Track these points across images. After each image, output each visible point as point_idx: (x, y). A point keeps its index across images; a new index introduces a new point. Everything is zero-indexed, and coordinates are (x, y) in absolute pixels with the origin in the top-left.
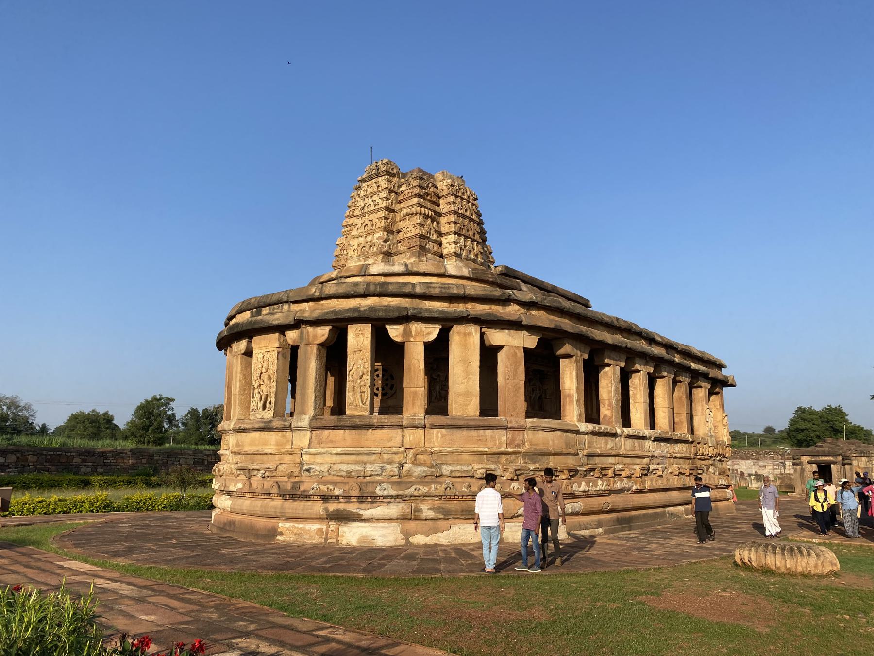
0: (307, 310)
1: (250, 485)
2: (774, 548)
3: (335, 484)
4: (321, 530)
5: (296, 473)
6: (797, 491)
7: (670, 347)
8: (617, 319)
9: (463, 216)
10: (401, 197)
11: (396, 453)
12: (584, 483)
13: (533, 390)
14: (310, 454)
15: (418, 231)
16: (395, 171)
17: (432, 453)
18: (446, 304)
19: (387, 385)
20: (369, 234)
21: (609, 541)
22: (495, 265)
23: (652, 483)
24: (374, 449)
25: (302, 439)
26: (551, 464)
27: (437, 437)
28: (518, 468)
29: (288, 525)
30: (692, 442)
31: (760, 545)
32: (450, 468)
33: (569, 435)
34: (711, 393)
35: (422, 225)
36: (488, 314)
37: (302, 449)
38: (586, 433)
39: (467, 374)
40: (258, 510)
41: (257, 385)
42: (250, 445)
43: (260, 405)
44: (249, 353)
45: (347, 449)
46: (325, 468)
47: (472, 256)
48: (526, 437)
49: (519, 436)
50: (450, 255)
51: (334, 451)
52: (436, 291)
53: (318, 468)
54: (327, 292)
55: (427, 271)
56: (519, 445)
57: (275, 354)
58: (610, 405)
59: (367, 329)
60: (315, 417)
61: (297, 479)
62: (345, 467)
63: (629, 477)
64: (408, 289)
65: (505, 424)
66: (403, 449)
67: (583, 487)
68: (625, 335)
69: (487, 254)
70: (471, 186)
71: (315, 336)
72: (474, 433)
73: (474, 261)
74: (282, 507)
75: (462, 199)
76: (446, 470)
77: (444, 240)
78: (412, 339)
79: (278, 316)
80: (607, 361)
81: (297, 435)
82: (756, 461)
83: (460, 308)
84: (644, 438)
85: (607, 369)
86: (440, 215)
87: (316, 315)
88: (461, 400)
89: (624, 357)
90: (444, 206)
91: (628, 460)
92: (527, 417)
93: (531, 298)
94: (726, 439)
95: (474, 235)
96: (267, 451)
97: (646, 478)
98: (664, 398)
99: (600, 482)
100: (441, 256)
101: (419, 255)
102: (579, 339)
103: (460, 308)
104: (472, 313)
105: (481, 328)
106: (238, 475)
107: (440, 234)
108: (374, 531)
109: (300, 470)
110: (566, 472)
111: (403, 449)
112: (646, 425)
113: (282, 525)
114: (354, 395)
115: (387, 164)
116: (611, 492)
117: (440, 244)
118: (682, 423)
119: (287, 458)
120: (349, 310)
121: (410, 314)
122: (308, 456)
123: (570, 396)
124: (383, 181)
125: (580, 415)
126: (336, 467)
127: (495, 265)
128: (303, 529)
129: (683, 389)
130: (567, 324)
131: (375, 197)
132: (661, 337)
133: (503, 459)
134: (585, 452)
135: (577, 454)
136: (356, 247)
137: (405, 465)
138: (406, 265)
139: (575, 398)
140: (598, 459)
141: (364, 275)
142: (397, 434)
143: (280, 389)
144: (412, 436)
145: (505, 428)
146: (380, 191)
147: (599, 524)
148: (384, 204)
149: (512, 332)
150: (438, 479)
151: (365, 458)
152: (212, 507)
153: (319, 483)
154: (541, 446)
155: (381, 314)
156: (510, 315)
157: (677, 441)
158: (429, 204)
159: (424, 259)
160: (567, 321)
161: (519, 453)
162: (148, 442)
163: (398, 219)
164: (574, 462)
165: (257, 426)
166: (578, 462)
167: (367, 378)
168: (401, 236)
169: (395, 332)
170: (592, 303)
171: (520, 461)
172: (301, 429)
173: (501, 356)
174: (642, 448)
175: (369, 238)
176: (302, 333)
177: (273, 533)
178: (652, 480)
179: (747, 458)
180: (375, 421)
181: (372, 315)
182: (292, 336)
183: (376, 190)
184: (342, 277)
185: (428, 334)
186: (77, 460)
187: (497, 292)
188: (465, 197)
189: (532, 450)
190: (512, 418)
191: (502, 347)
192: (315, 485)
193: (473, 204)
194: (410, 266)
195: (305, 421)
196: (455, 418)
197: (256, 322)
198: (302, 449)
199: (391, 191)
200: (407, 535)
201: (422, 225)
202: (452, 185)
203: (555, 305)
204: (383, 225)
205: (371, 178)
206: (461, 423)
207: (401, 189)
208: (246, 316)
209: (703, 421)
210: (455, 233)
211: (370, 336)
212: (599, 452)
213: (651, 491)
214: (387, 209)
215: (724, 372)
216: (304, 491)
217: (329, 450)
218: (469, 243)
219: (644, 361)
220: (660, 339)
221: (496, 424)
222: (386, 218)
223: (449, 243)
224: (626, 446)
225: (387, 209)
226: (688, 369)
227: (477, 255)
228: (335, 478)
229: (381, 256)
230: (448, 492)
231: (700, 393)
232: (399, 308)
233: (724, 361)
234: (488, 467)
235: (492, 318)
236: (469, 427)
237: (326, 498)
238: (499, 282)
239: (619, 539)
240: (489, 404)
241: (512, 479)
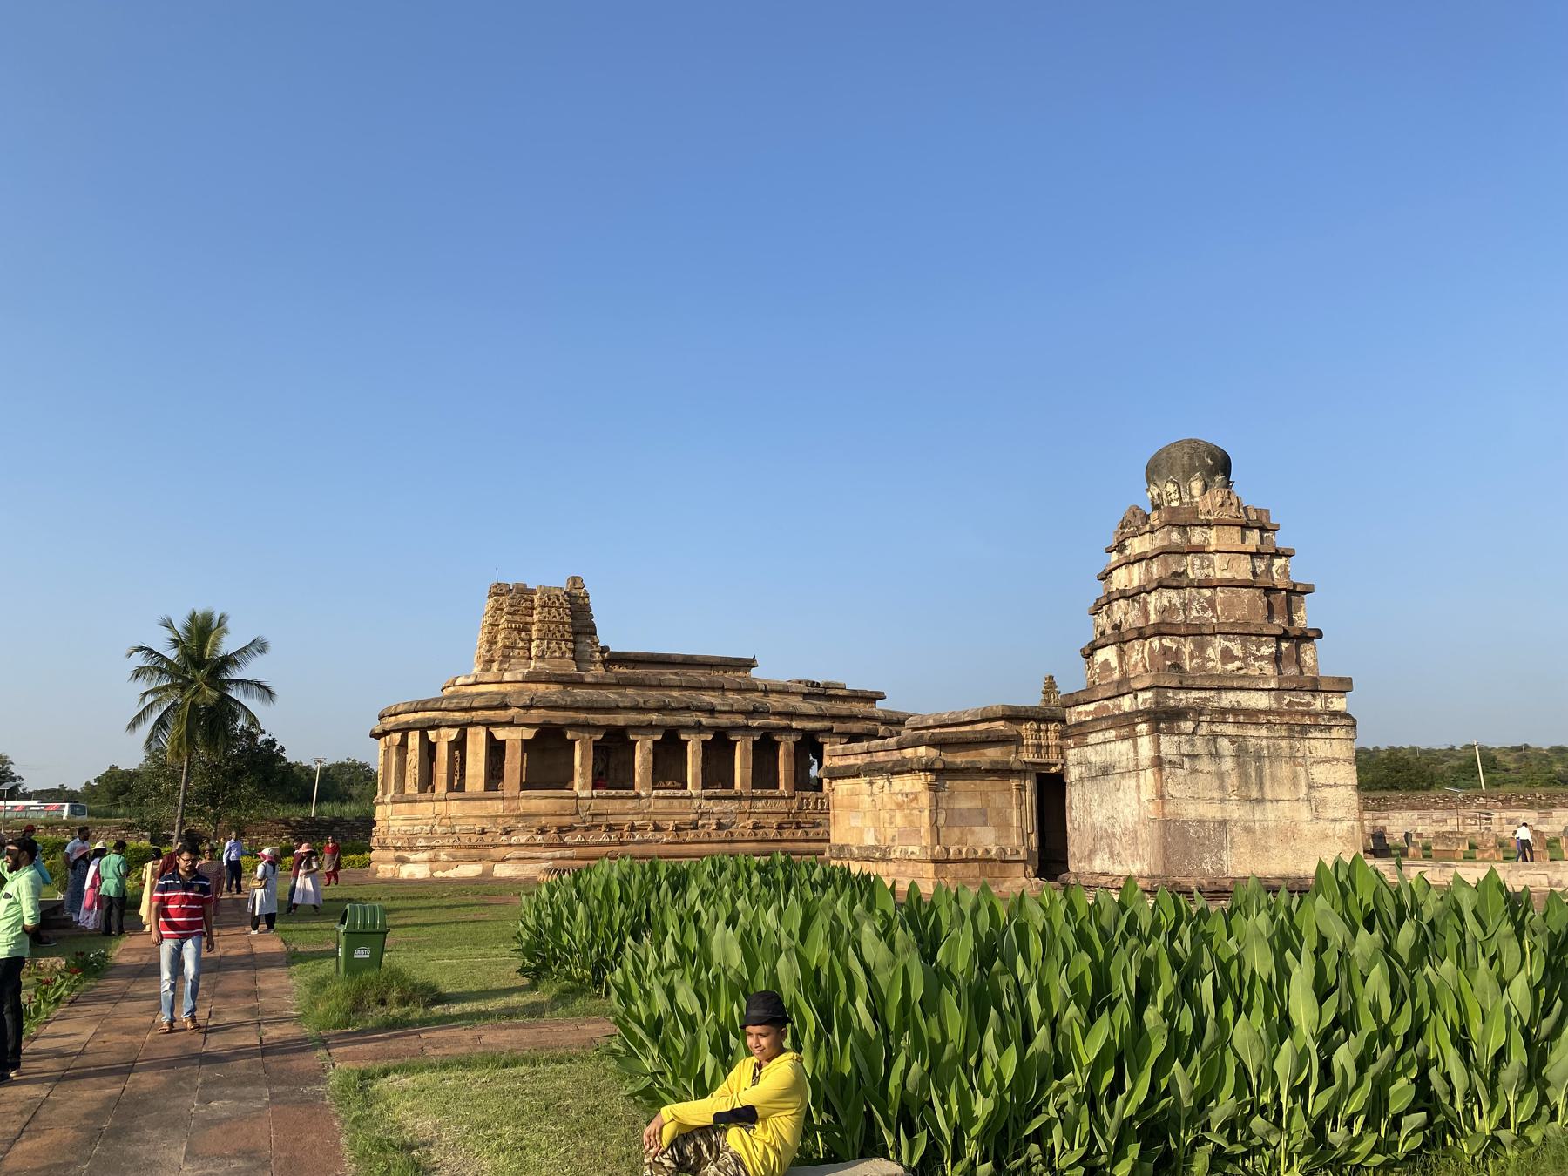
0: (391, 722)
39: (475, 761)
49: (514, 805)
73: (562, 657)
76: (457, 829)
84: (691, 797)
100: (530, 658)
108: (416, 870)
112: (695, 786)
113: (381, 867)
116: (622, 843)
135: (577, 813)
144: (440, 807)
158: (518, 618)
169: (432, 735)
171: (513, 822)
177: (377, 871)
195: (388, 799)
214: (492, 625)
218: (553, 645)
225: (492, 625)
226: (789, 729)
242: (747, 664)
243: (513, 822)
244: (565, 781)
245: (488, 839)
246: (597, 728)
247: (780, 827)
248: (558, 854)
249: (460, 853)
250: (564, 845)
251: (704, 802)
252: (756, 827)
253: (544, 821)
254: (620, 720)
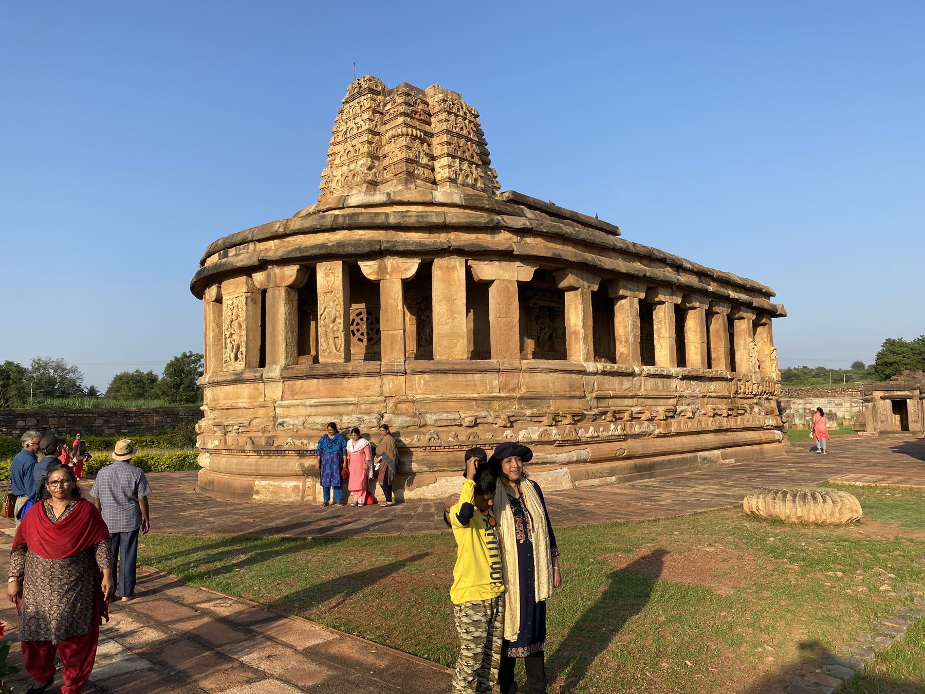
0: (272, 249)
1: (226, 441)
2: (785, 494)
3: (310, 437)
4: (297, 487)
5: (270, 428)
6: (869, 429)
7: (702, 274)
8: (634, 245)
9: (459, 136)
10: (387, 118)
11: (374, 403)
12: (592, 428)
13: (541, 329)
14: (283, 407)
15: (404, 155)
16: (379, 88)
17: (414, 401)
18: (426, 235)
19: (372, 329)
20: (352, 162)
21: (618, 491)
22: (501, 191)
23: (679, 425)
24: (351, 399)
25: (275, 391)
26: (552, 408)
27: (419, 382)
28: (511, 414)
29: (264, 483)
30: (731, 380)
31: (770, 491)
32: (434, 417)
33: (574, 376)
34: (756, 325)
35: (408, 148)
36: (473, 245)
37: (275, 402)
38: (596, 373)
39: (452, 312)
40: (234, 468)
41: (228, 334)
42: (225, 399)
43: (232, 355)
44: (219, 300)
45: (321, 400)
46: (299, 422)
47: (470, 181)
48: (522, 380)
49: (513, 380)
50: (444, 181)
51: (308, 402)
52: (412, 221)
53: (291, 422)
54: (292, 228)
55: (411, 200)
56: (513, 390)
57: (243, 300)
58: (627, 341)
59: (337, 267)
60: (286, 368)
61: (272, 434)
63: (651, 420)
64: (380, 220)
65: (497, 366)
66: (382, 398)
67: (591, 432)
68: (645, 262)
69: (491, 180)
70: (470, 101)
71: (283, 278)
72: (461, 378)
73: (473, 187)
74: (256, 465)
75: (457, 116)
76: (430, 419)
77: (437, 165)
78: (388, 277)
79: (240, 257)
80: (621, 292)
81: (268, 386)
82: (832, 399)
83: (442, 239)
84: (669, 377)
85: (623, 301)
86: (432, 135)
87: (280, 253)
88: (445, 342)
89: (644, 287)
90: (436, 125)
91: (650, 402)
92: (522, 359)
93: (524, 224)
94: (774, 376)
95: (472, 156)
96: (240, 405)
97: (672, 421)
98: (695, 332)
99: (612, 426)
100: (434, 182)
101: (406, 182)
102: (584, 268)
103: (442, 239)
104: (453, 243)
105: (467, 261)
106: (216, 432)
107: (432, 158)
109: (274, 425)
110: (569, 416)
111: (382, 398)
112: (672, 361)
113: (259, 483)
114: (327, 341)
115: (370, 80)
116: (626, 437)
117: (433, 170)
118: (719, 358)
119: (261, 412)
120: (315, 247)
121: (382, 248)
122: (281, 409)
123: (576, 333)
124: (365, 101)
125: (588, 354)
126: (311, 420)
127: (501, 191)
128: (279, 487)
129: (720, 321)
130: (569, 252)
131: (358, 120)
132: (691, 263)
133: (496, 405)
134: (594, 395)
135: (585, 397)
136: (339, 177)
137: (385, 415)
138: (388, 194)
139: (582, 334)
140: (611, 402)
141: (343, 208)
142: (374, 383)
143: (251, 338)
144: (390, 384)
145: (498, 371)
146: (363, 112)
147: (612, 472)
148: (367, 127)
149: (503, 263)
150: (421, 429)
151: (342, 409)
152: (198, 467)
153: (293, 437)
154: (540, 390)
155: (351, 250)
156: (500, 243)
157: (711, 379)
158: (417, 123)
159: (413, 186)
160: (570, 248)
161: (514, 398)
162: (181, 401)
163: (384, 143)
164: (580, 406)
165: (229, 378)
166: (589, 405)
167: (340, 321)
168: (387, 161)
169: (368, 269)
170: (621, 230)
171: (515, 407)
172: (273, 380)
173: (492, 291)
174: (667, 389)
175: (352, 166)
176: (269, 275)
177: (249, 492)
178: (679, 423)
179: (822, 396)
180: (350, 369)
181: (341, 251)
182: (259, 277)
183: (359, 111)
184: (319, 211)
185: (406, 270)
186: (99, 422)
187: (483, 218)
188: (461, 113)
189: (529, 394)
190: (505, 360)
191: (493, 281)
192: (289, 440)
193: (470, 122)
194: (392, 195)
196: (439, 362)
197: (221, 265)
198: (275, 402)
199: (375, 112)
201: (408, 148)
202: (444, 101)
203: (553, 230)
204: (366, 150)
205: (353, 98)
206: (446, 367)
207: (387, 108)
208: (214, 259)
209: (746, 356)
210: (449, 155)
211: (341, 274)
212: (611, 393)
213: (679, 434)
215: (772, 300)
216: (278, 446)
217: (302, 401)
218: (465, 166)
219: (670, 291)
220: (689, 266)
221: (487, 367)
222: (370, 143)
223: (442, 167)
224: (646, 386)
226: (727, 299)
227: (476, 180)
228: (311, 431)
229: (365, 185)
230: (432, 443)
231: (742, 326)
232: (370, 242)
233: (772, 288)
234: (477, 414)
235: (478, 249)
236: (455, 372)
237: (301, 453)
238: (497, 209)
239: (633, 487)
240: (481, 347)
241: (505, 427)
242: (614, 232)
243: (515, 407)
247: (729, 415)
248: (574, 453)
249: (440, 457)
250: (577, 442)
252: (715, 415)
253: (553, 406)
254: (621, 265)
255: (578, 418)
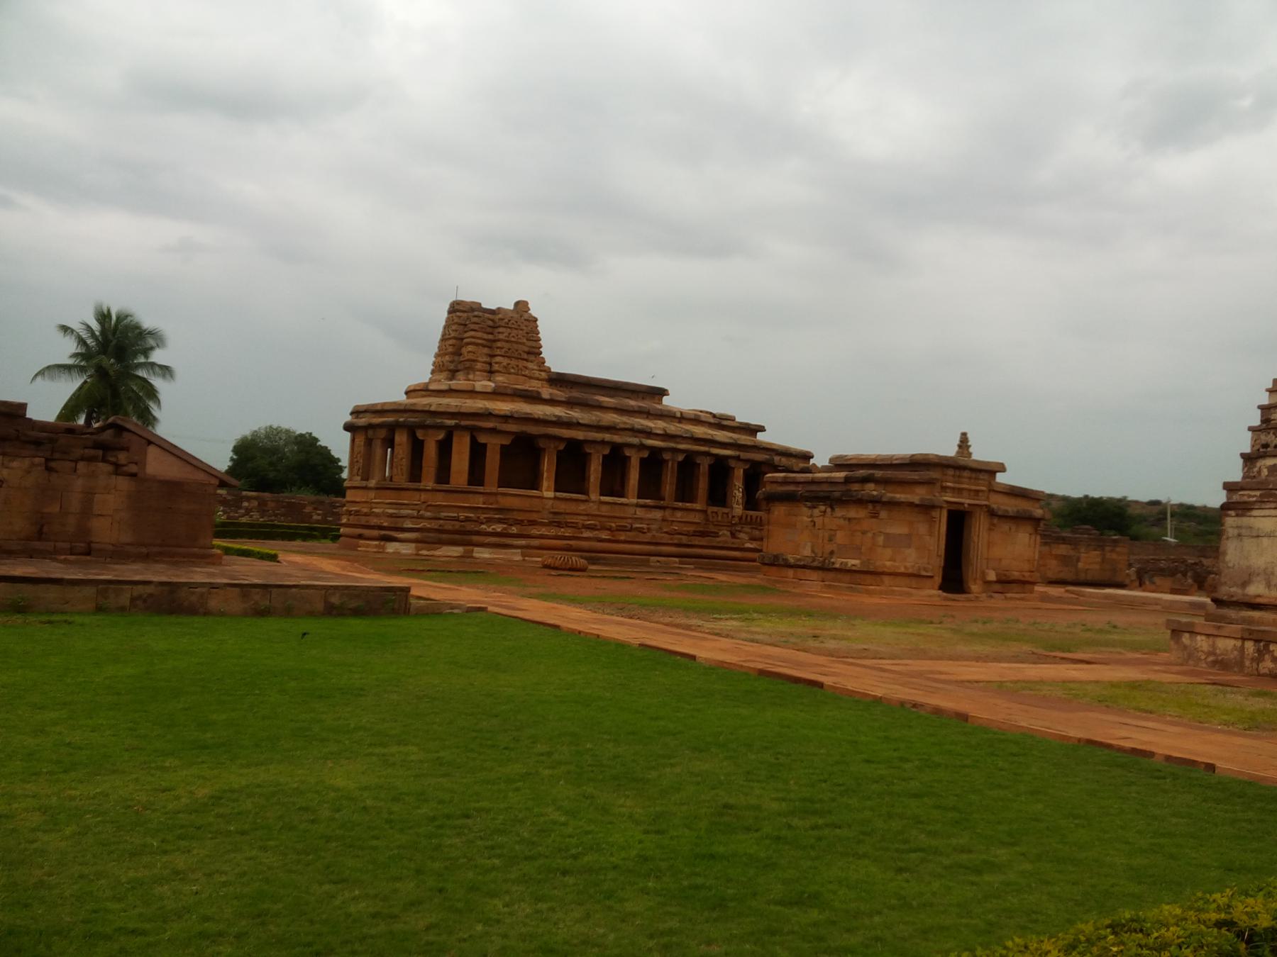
25: (372, 494)
62: (390, 511)
79: (362, 421)
142: (417, 494)
158: (479, 334)
169: (420, 434)
182: (370, 433)
200: (418, 549)
226: (707, 454)
237: (381, 528)
244: (535, 484)
245: (470, 526)
246: (560, 439)
249: (444, 536)
251: (638, 510)
254: (579, 435)
255: (533, 523)
